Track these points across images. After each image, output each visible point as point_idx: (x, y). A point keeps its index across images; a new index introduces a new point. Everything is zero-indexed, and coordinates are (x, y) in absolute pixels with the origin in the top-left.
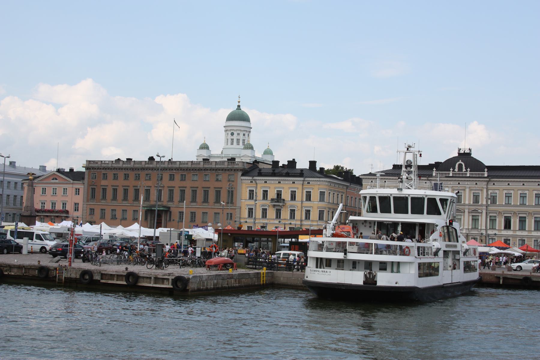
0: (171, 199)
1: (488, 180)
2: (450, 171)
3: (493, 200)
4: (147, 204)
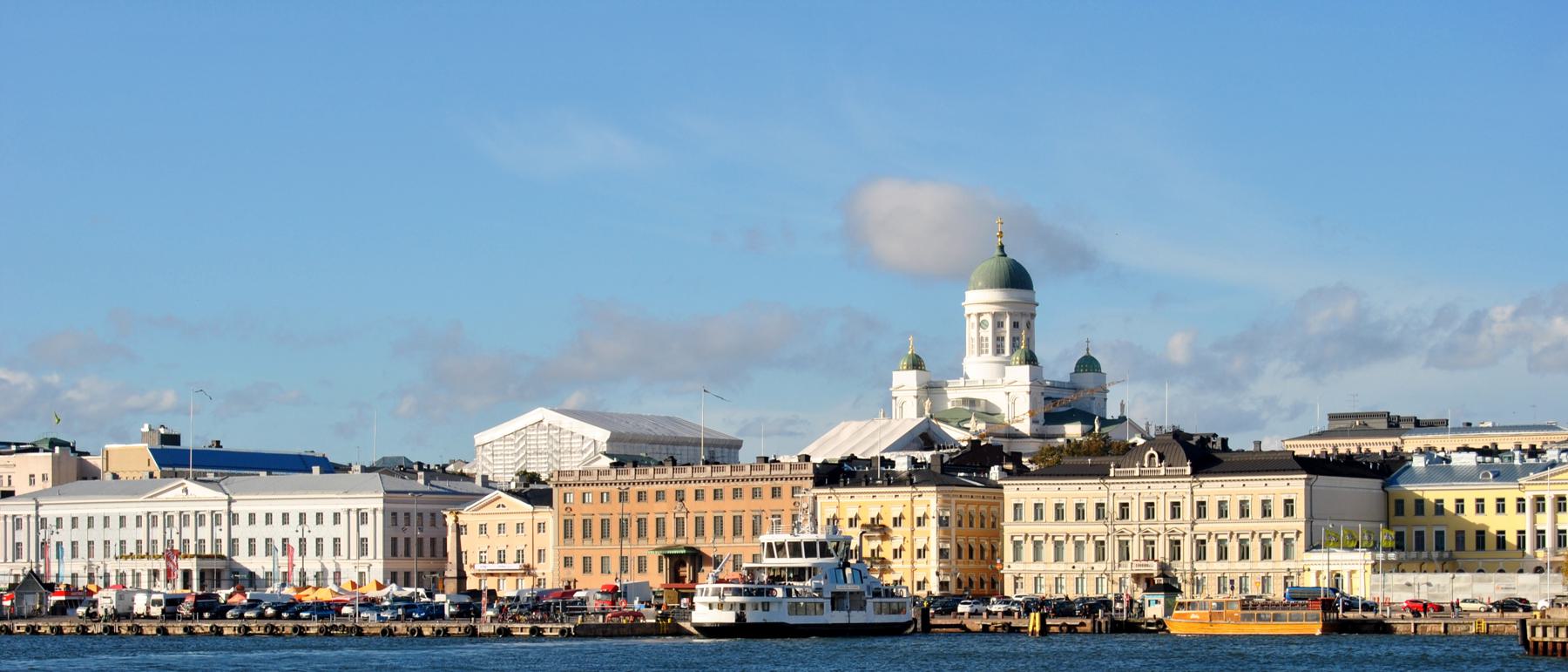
0: (700, 532)
1: (1190, 479)
2: (1134, 466)
3: (1201, 508)
4: (661, 543)
